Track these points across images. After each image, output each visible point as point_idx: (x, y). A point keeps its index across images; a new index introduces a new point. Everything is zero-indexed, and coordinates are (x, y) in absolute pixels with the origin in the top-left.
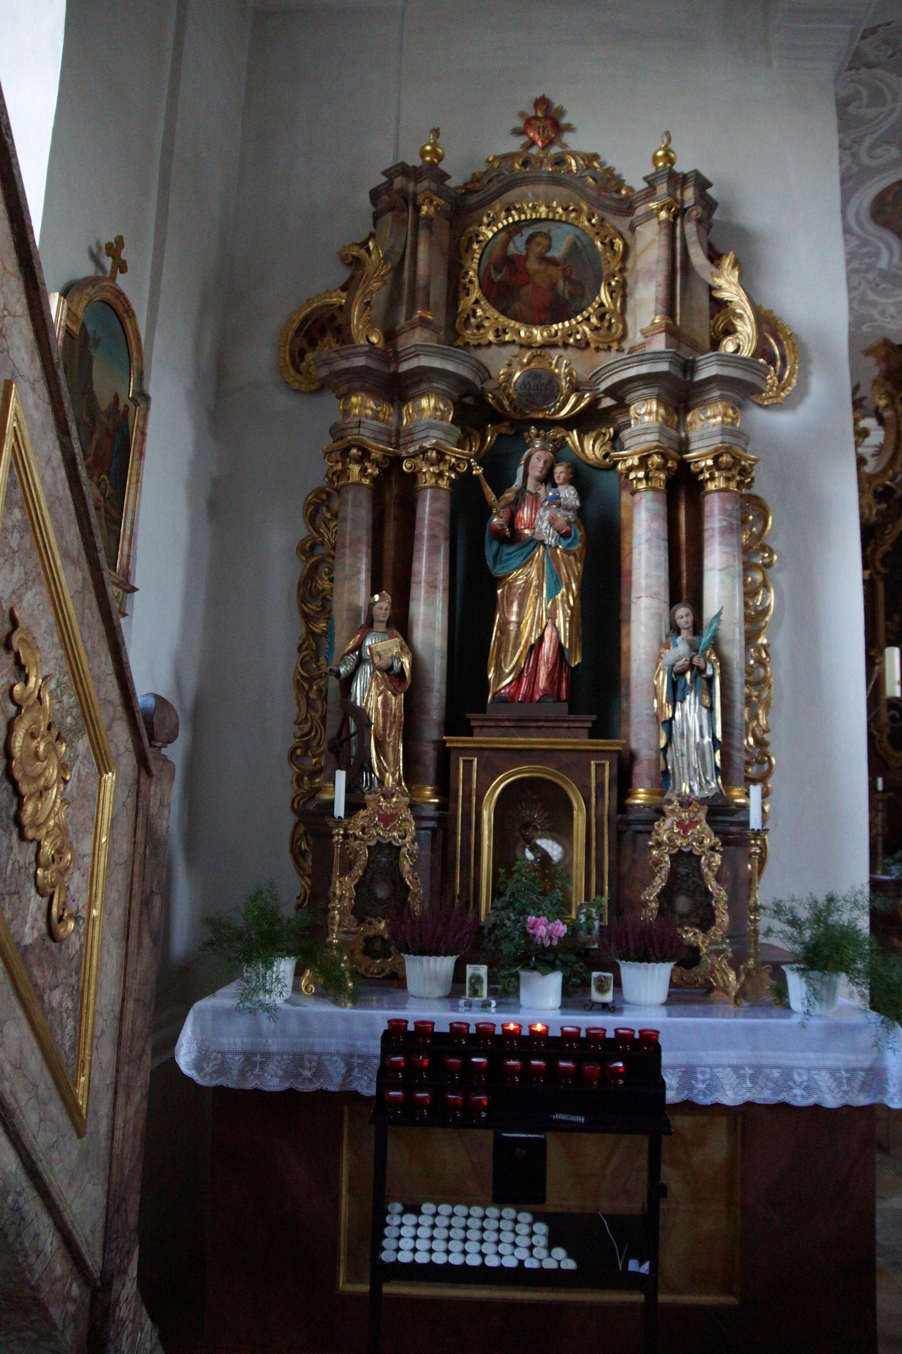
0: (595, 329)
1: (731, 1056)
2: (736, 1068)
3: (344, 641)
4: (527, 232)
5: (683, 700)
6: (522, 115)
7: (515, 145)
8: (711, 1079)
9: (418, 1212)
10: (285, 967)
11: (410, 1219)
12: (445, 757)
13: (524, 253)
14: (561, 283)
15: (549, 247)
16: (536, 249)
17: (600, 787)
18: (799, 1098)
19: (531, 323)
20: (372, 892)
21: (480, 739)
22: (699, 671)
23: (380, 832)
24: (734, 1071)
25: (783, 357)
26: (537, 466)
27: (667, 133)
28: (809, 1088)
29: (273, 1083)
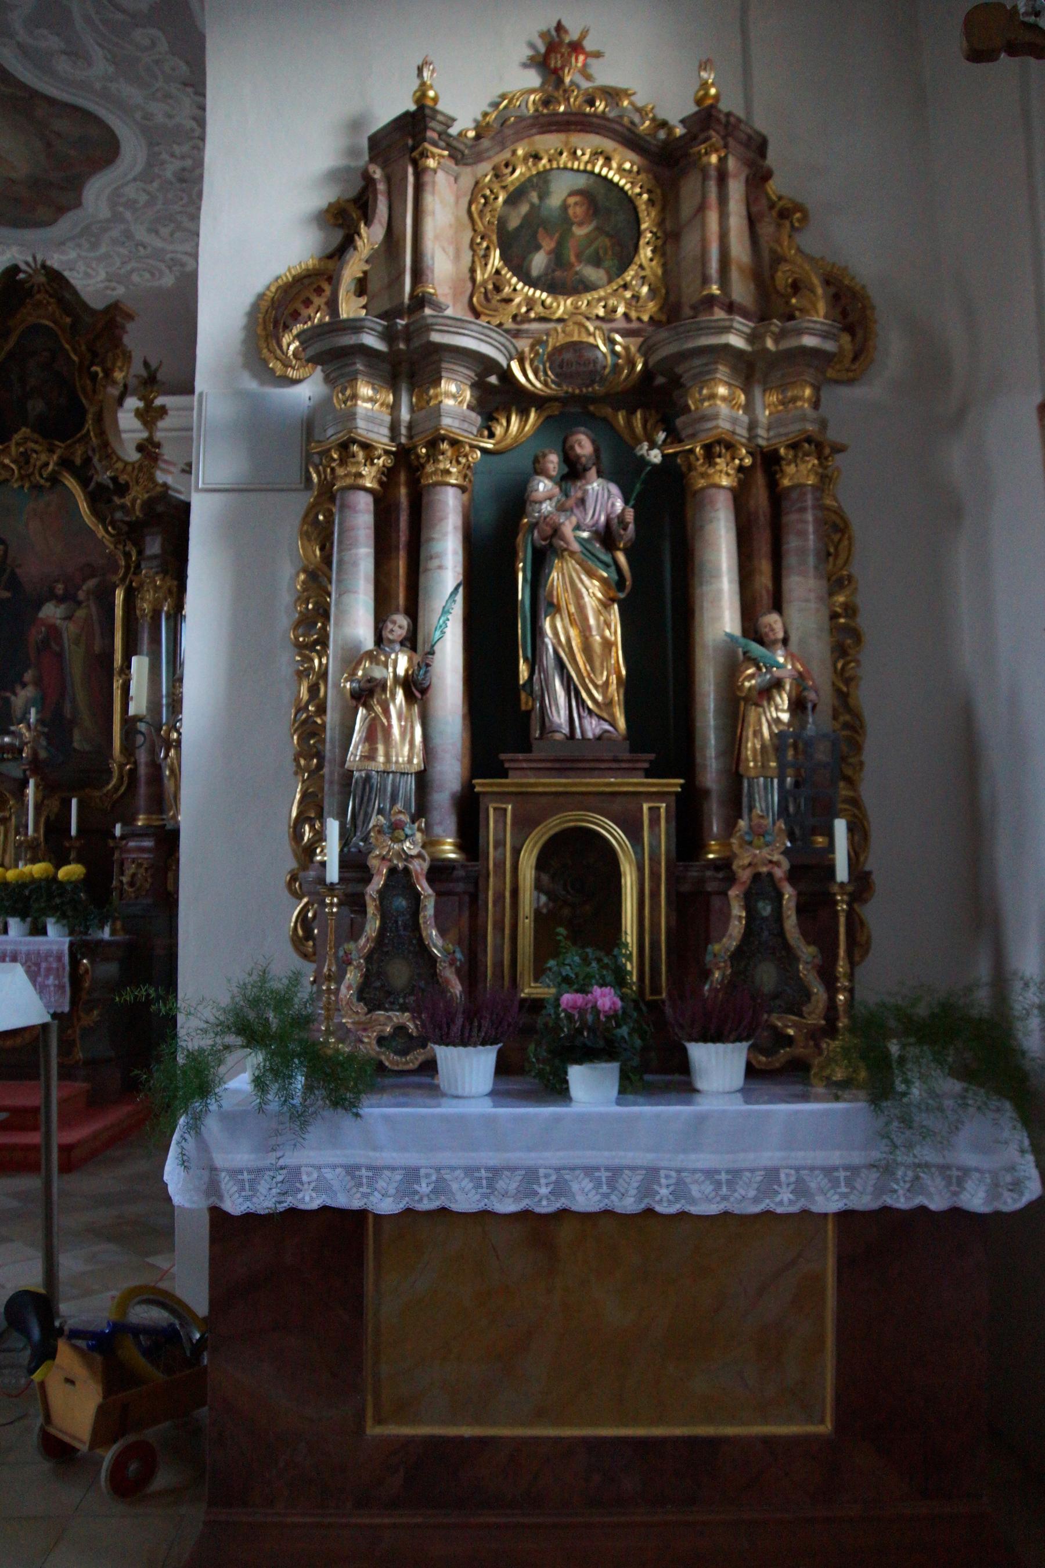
8: (437, 1181)
24: (348, 1174)
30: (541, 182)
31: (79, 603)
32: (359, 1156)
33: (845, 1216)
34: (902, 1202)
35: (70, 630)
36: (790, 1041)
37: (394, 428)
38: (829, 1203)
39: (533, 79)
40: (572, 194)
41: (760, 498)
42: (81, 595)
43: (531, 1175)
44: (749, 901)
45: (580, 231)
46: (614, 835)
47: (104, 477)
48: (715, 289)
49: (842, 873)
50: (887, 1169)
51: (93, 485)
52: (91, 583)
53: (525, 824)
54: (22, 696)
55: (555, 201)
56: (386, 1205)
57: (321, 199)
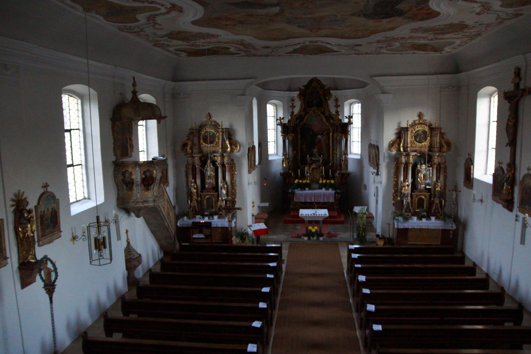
0: (216, 145)
1: (220, 223)
3: (190, 184)
7: (205, 119)
10: (185, 218)
18: (225, 226)
21: (204, 193)
22: (224, 187)
23: (194, 204)
27: (222, 122)
29: (185, 226)
30: (418, 131)
31: (324, 135)
32: (408, 224)
33: (442, 229)
34: (446, 228)
35: (323, 140)
36: (438, 216)
37: (405, 160)
38: (441, 228)
39: (417, 118)
40: (422, 132)
41: (438, 167)
42: (324, 134)
43: (420, 226)
44: (436, 205)
45: (422, 136)
46: (423, 197)
47: (327, 114)
48: (436, 146)
49: (443, 204)
50: (445, 226)
51: (325, 116)
52: (326, 132)
53: (416, 197)
54: (315, 150)
55: (420, 132)
56: (410, 227)
57: (396, 132)
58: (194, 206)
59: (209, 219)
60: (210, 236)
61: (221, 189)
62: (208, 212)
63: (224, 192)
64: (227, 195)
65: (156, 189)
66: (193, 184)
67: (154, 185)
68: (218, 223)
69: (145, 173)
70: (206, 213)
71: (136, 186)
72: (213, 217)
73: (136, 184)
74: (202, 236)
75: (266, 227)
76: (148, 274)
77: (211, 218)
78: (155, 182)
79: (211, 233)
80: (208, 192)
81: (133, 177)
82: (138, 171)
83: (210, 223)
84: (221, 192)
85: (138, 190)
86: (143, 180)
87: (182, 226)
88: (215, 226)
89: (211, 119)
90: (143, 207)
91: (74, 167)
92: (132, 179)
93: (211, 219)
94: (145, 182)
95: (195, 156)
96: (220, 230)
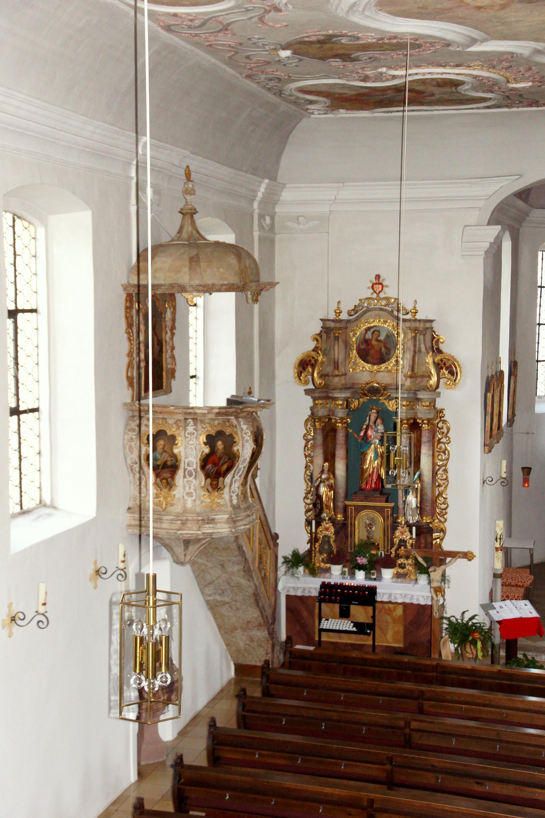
2: (401, 595)
4: (372, 330)
5: (409, 494)
6: (371, 281)
7: (368, 293)
9: (328, 620)
10: (301, 569)
11: (326, 621)
12: (345, 508)
13: (371, 338)
14: (383, 349)
15: (379, 336)
16: (375, 336)
17: (388, 516)
18: (415, 602)
19: (374, 364)
20: (323, 547)
25: (457, 373)
26: (373, 418)
28: (417, 600)
58: (325, 537)
59: (367, 578)
60: (372, 626)
61: (406, 493)
62: (365, 557)
63: (412, 500)
64: (421, 509)
65: (238, 488)
66: (324, 476)
67: (233, 477)
68: (394, 592)
69: (211, 440)
70: (362, 561)
71: (185, 477)
72: (380, 572)
73: (185, 470)
74: (347, 625)
75: (535, 614)
76: (203, 731)
77: (373, 574)
78: (238, 467)
79: (374, 617)
80: (366, 499)
81: (176, 451)
82: (194, 434)
83: (373, 591)
84: (404, 502)
85: (190, 488)
86: (205, 461)
87: (292, 593)
88: (386, 599)
89: (385, 293)
90: (201, 537)
91: (22, 416)
92: (175, 457)
93: (375, 579)
94: (209, 466)
95: (336, 395)
96: (399, 611)
